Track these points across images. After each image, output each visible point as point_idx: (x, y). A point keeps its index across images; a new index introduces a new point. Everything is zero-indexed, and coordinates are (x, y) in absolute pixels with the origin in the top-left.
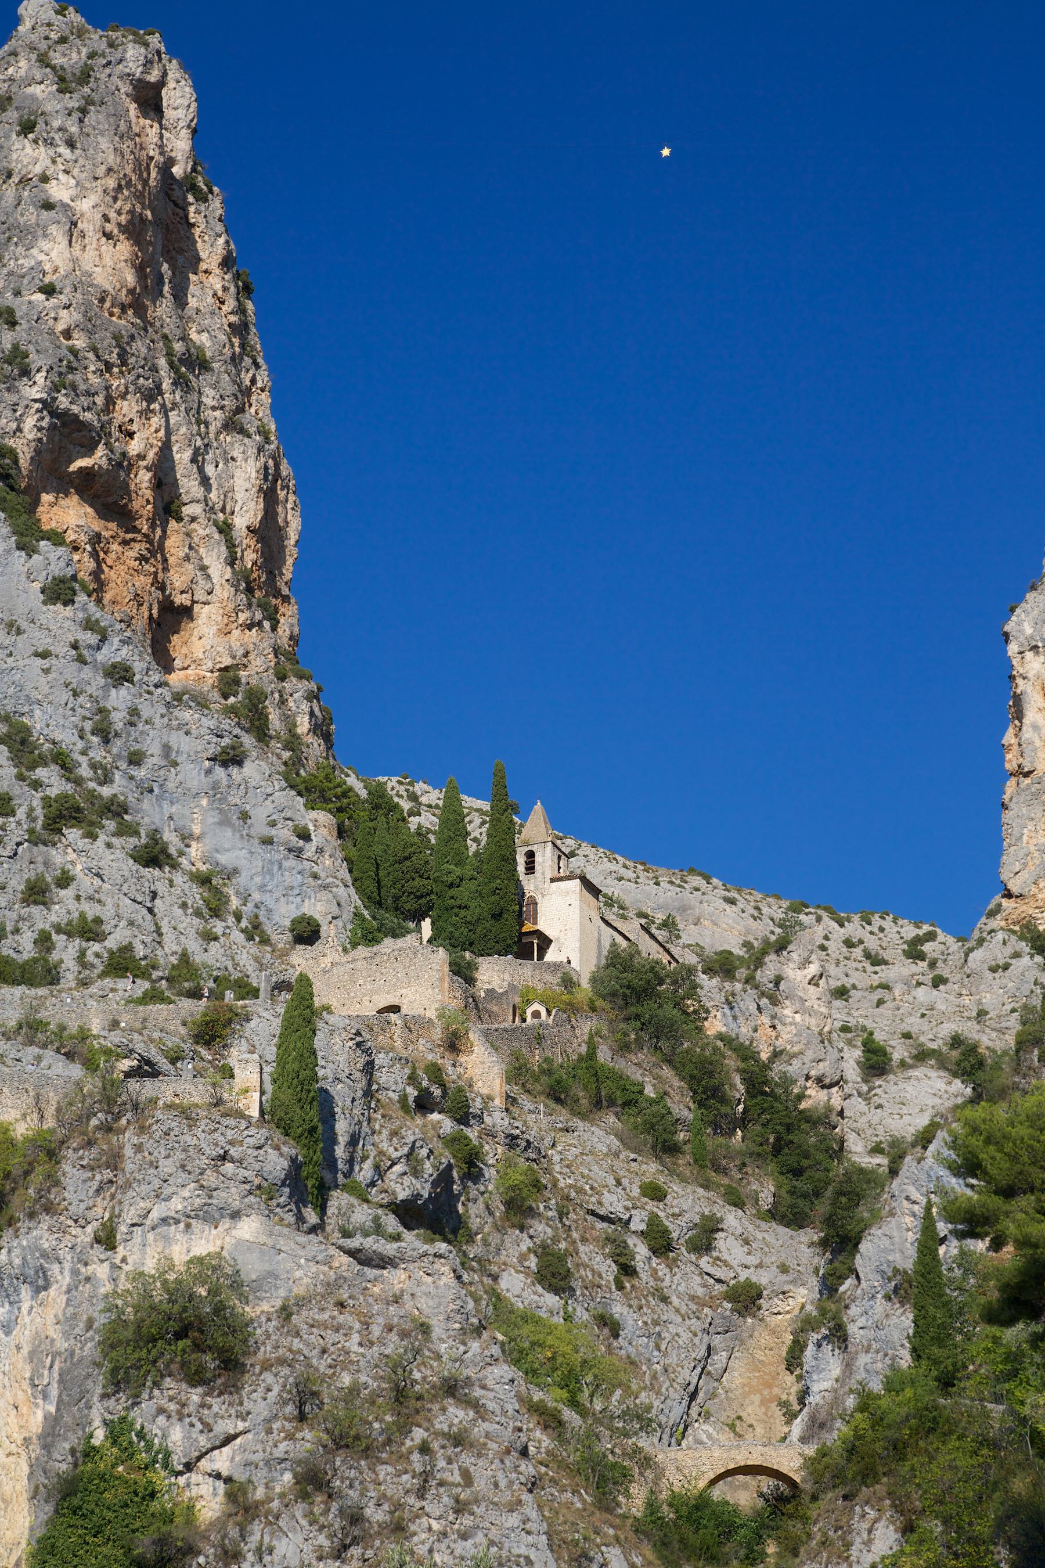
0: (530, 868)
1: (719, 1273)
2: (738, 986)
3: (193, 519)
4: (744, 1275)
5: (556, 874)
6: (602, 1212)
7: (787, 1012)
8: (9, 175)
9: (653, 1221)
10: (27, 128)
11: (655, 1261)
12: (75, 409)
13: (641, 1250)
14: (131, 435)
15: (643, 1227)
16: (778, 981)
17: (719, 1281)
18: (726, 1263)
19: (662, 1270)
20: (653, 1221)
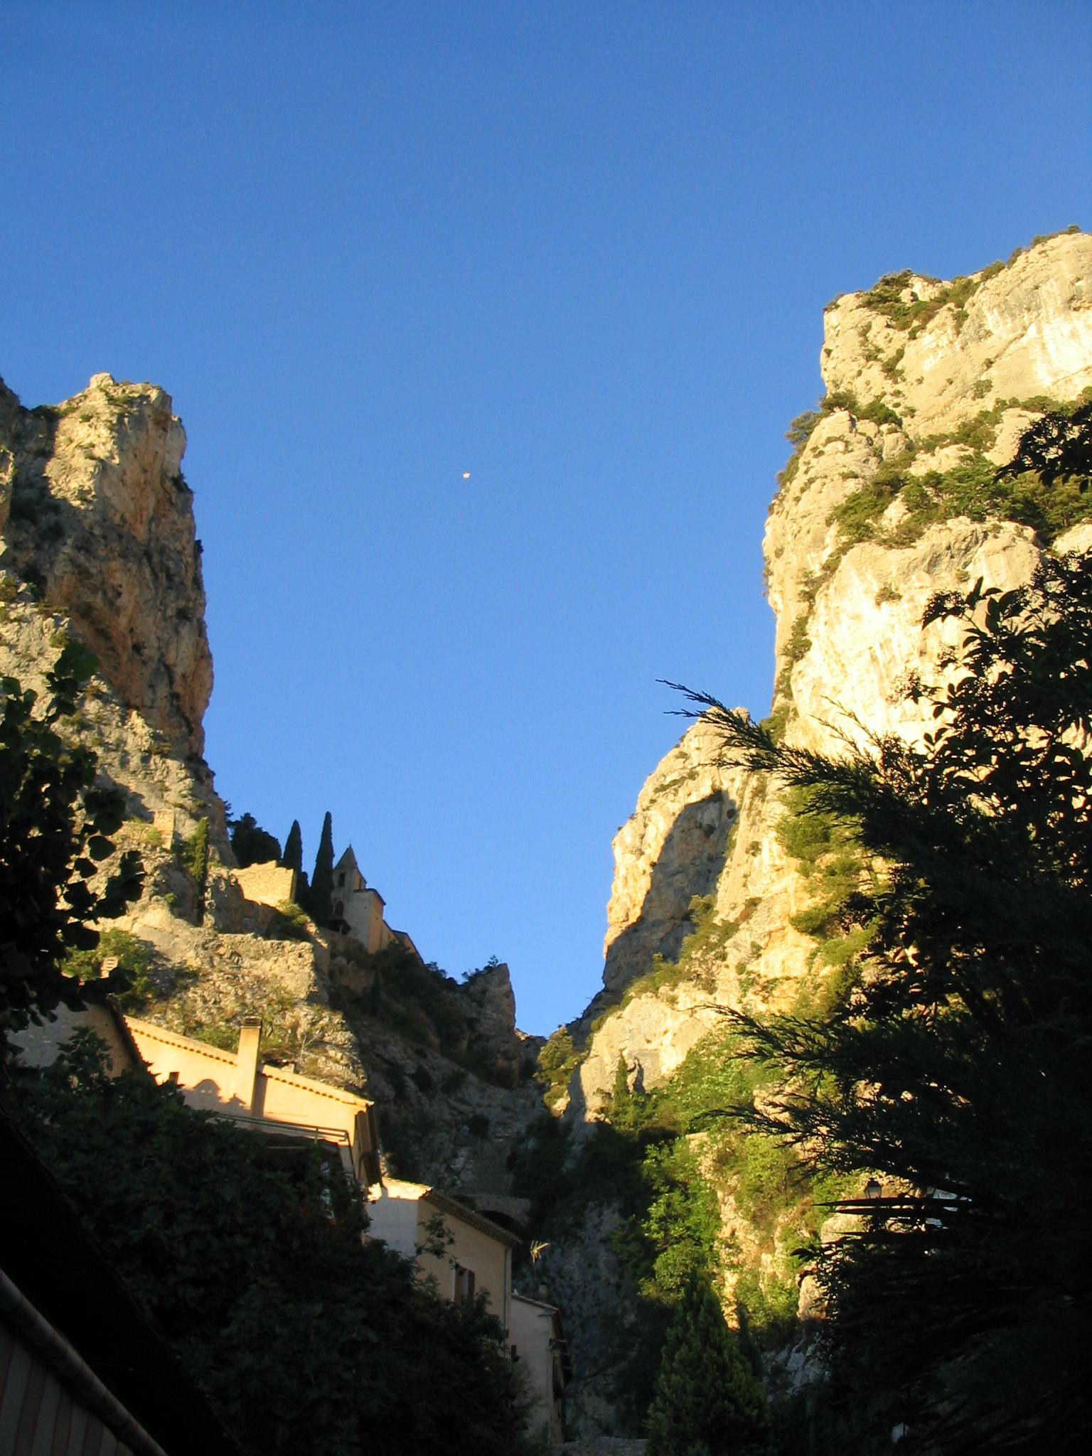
0: (341, 883)
1: (463, 1108)
2: (458, 995)
3: (151, 659)
4: (479, 1111)
5: (357, 888)
6: (387, 1056)
7: (488, 1012)
8: (71, 441)
9: (420, 1069)
10: (87, 418)
11: (420, 1094)
12: (87, 564)
13: (411, 1084)
14: (119, 594)
15: (413, 1071)
16: (484, 992)
17: (461, 1113)
18: (468, 1104)
19: (424, 1100)
20: (420, 1069)
